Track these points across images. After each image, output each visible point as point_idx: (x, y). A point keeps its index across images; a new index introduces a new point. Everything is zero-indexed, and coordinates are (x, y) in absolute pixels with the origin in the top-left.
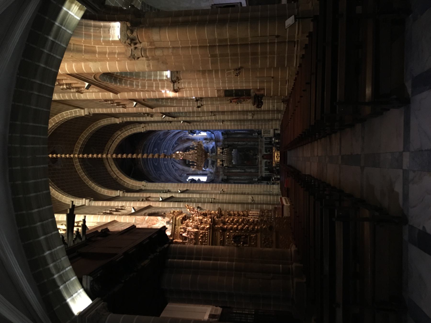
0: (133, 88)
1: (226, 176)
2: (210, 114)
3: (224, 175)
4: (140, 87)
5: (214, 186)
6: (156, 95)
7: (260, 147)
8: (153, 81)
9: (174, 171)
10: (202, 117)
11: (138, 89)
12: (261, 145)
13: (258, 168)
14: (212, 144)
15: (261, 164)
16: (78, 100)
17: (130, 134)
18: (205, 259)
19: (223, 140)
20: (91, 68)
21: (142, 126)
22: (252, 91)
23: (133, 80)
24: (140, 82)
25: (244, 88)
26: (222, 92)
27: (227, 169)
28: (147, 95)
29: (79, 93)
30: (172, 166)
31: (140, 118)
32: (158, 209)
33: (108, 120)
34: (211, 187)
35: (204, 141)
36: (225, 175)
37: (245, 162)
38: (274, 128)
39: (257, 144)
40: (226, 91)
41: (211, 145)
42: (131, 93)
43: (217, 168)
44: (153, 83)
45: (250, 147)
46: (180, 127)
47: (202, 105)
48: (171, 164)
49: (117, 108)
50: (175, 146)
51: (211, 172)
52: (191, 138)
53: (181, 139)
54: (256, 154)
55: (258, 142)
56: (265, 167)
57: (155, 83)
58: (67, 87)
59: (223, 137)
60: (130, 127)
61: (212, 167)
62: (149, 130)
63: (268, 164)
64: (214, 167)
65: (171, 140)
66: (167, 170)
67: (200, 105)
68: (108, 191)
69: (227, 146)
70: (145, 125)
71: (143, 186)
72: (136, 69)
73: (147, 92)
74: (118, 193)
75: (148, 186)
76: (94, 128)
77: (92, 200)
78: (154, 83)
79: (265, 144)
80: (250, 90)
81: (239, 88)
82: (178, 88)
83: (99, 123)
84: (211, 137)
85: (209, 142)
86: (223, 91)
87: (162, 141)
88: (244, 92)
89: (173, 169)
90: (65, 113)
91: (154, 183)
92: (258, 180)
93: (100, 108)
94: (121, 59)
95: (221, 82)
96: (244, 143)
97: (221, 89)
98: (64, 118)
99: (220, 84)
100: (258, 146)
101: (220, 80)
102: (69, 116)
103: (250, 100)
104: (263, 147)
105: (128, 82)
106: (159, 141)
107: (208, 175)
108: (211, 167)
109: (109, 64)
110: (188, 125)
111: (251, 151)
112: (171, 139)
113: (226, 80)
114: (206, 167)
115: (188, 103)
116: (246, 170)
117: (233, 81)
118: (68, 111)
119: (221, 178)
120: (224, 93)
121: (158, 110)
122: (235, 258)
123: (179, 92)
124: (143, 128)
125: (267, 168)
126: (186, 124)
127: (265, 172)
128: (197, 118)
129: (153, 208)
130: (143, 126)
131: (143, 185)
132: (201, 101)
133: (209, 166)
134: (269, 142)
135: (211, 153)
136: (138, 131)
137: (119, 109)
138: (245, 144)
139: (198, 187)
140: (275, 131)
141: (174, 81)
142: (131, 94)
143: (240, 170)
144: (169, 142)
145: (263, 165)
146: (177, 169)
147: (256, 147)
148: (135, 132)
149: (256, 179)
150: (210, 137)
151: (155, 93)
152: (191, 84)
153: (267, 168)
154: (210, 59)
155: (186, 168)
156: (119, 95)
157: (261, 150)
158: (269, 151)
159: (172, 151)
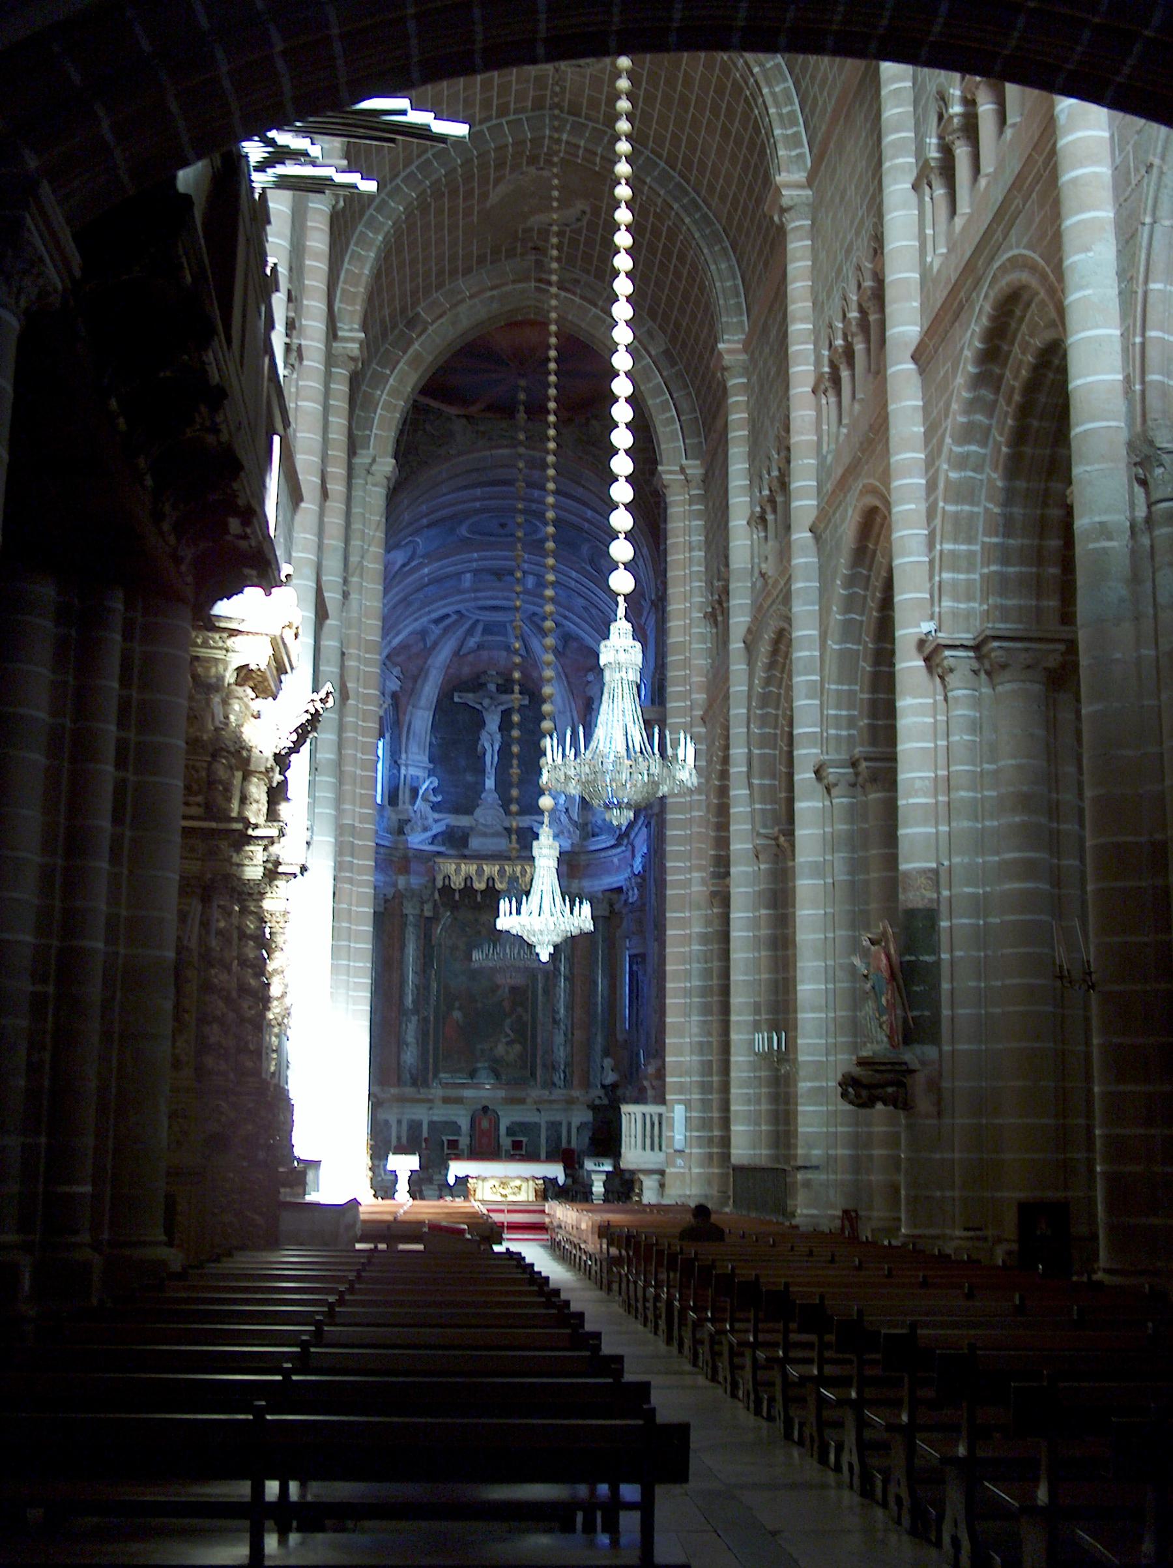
0: (948, 440)
2: (762, 831)
4: (953, 475)
5: (360, 843)
6: (910, 554)
7: (535, 1093)
8: (983, 543)
9: (416, 625)
10: (750, 786)
11: (945, 466)
12: (551, 1102)
15: (446, 1100)
16: (880, 163)
17: (650, 402)
18: (120, 788)
20: (1088, 250)
21: (690, 467)
22: (930, 1052)
23: (991, 441)
24: (979, 477)
25: (946, 1012)
26: (923, 897)
27: (421, 916)
28: (913, 506)
29: (914, 174)
30: (447, 616)
31: (746, 456)
32: (285, 540)
33: (738, 296)
34: (357, 824)
36: (386, 901)
37: (457, 1015)
38: (668, 1171)
39: (556, 1079)
40: (930, 916)
42: (922, 430)
43: (427, 858)
44: (976, 544)
45: (539, 1040)
46: (686, 663)
47: (828, 790)
48: (458, 612)
49: (817, 350)
51: (407, 829)
54: (497, 1075)
55: (568, 1083)
56: (432, 1124)
57: (972, 554)
58: (956, 120)
60: (685, 405)
61: (434, 832)
62: (668, 500)
63: (444, 1138)
64: (432, 843)
65: (585, 615)
66: (427, 585)
67: (831, 779)
68: (364, 280)
70: (694, 484)
71: (368, 461)
72: (1088, 468)
73: (923, 507)
74: (351, 330)
75: (369, 487)
76: (695, 222)
77: (337, 202)
78: (973, 548)
79: (554, 1126)
80: (935, 1040)
81: (945, 986)
82: (951, 670)
83: (717, 248)
84: (597, 830)
85: (570, 818)
86: (931, 900)
87: (589, 568)
88: (927, 1013)
89: (425, 619)
90: (787, 90)
91: (384, 520)
93: (815, 260)
94: (1138, 397)
95: (981, 891)
96: (562, 1011)
97: (939, 893)
98: (762, 84)
99: (967, 885)
100: (543, 1088)
101: (988, 889)
102: (772, 111)
103: (885, 1039)
104: (538, 1110)
105: (979, 418)
106: (585, 549)
108: (437, 829)
109: (1111, 336)
110: (691, 708)
111: (517, 1047)
112: (594, 611)
113: (991, 920)
115: (844, 713)
116: (414, 1019)
117: (986, 956)
118: (797, 107)
120: (920, 906)
121: (804, 558)
122: (122, 951)
123: (924, 671)
124: (682, 470)
125: (425, 1134)
126: (700, 697)
127: (399, 1122)
128: (744, 760)
129: (289, 515)
130: (688, 472)
131: (374, 460)
132: (853, 785)
133: (437, 816)
134: (564, 1145)
135: (506, 829)
136: (663, 446)
137: (812, 359)
139: (359, 755)
140: (656, 1177)
141: (985, 650)
142: (915, 429)
144: (582, 602)
145: (441, 1113)
146: (428, 645)
147: (539, 1072)
148: (660, 429)
151: (923, 548)
152: (966, 737)
153: (425, 1134)
154: (1143, 839)
155: (430, 690)
156: (911, 366)
157: (522, 1101)
158: (517, 1145)
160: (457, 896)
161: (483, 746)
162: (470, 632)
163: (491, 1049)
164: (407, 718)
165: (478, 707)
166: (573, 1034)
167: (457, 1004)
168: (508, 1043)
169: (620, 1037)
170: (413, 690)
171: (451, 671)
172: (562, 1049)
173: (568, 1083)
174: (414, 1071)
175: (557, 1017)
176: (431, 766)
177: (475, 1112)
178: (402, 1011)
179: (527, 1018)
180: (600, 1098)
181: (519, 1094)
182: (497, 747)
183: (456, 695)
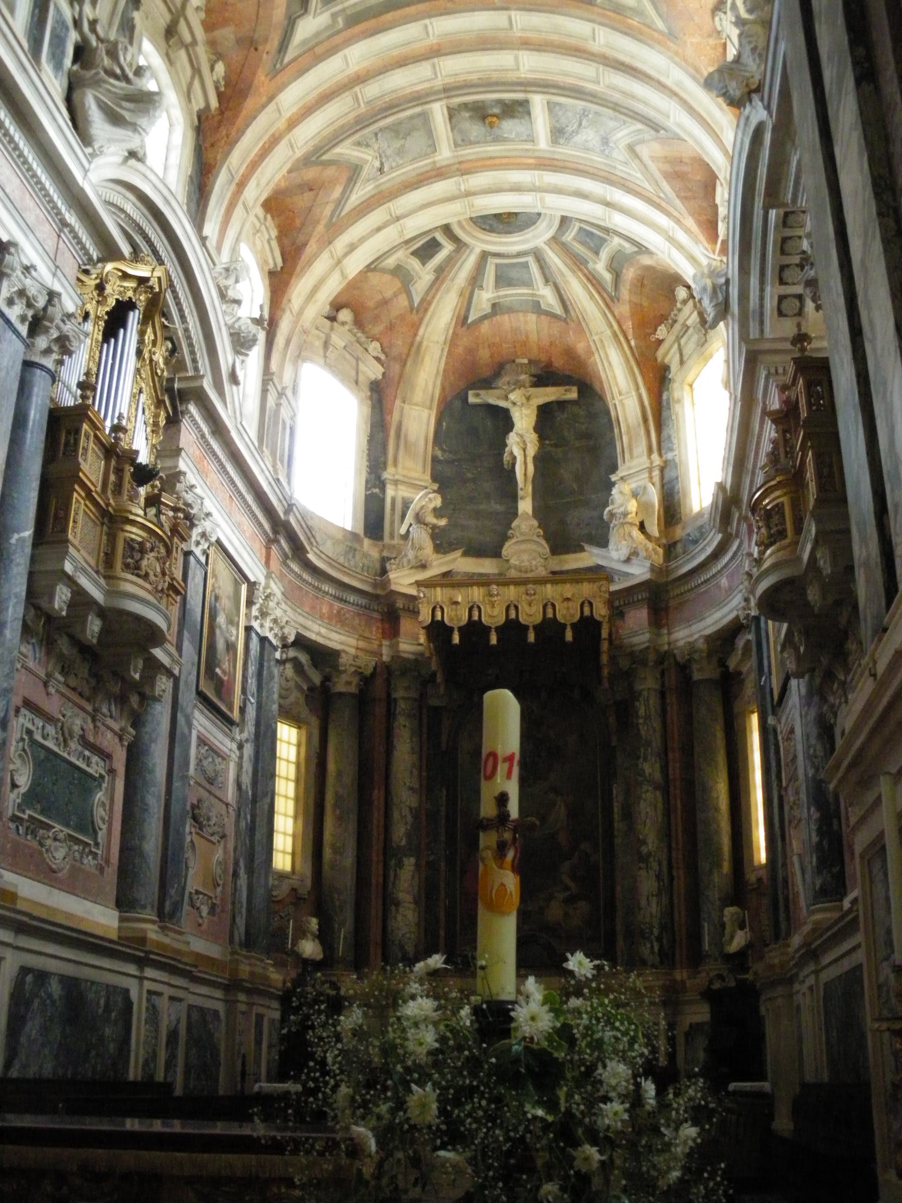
1: (353, 689)
3: (368, 672)
14: (628, 560)
35: (654, 495)
41: (624, 553)
48: (447, 229)
50: (600, 266)
52: (676, 395)
53: (662, 318)
59: (701, 645)
92: (308, 966)
107: (367, 542)
111: (583, 906)
114: (431, 519)
116: (409, 863)
138: (644, 842)
146: (417, 300)
149: (309, 948)
159: (556, 240)
161: (511, 453)
162: (476, 280)
164: (396, 416)
165: (502, 404)
166: (671, 879)
168: (570, 900)
169: (752, 877)
170: (401, 376)
171: (460, 350)
172: (654, 901)
173: (667, 959)
175: (644, 850)
176: (436, 486)
178: (389, 852)
180: (721, 977)
182: (532, 451)
183: (471, 393)
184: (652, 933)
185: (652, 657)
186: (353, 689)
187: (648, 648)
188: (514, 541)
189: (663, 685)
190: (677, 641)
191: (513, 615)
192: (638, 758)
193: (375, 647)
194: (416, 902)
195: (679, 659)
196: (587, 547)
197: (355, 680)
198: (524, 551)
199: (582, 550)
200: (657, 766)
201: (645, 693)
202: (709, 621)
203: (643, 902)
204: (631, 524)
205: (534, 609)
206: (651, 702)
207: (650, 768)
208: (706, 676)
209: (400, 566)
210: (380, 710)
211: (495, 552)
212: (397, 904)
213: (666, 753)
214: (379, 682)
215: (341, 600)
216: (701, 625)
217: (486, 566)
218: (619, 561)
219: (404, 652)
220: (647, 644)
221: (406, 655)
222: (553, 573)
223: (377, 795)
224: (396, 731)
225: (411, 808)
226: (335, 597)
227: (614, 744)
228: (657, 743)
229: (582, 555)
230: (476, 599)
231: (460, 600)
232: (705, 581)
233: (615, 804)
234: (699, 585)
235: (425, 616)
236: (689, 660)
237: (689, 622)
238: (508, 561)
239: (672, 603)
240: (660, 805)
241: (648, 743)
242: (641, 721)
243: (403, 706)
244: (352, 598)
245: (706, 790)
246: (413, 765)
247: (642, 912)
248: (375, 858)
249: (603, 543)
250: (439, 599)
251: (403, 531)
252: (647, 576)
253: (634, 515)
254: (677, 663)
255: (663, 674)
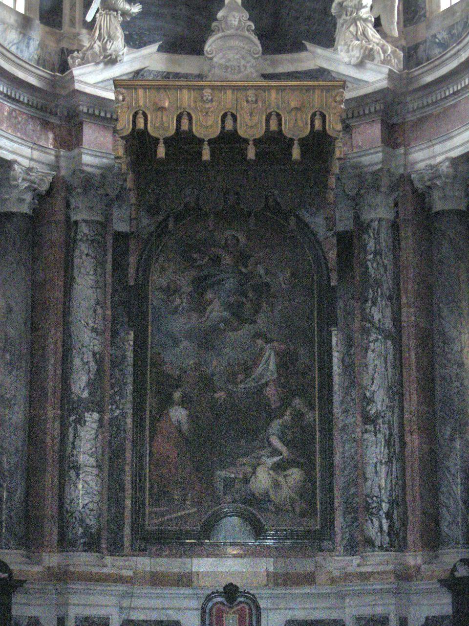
1: (25, 209)
3: (44, 188)
12: (364, 577)
13: (116, 548)
14: (360, 65)
19: (405, 180)
37: (178, 414)
59: (445, 168)
69: (340, 227)
100: (352, 548)
111: (295, 475)
119: (9, 157)
138: (370, 401)
143: (99, 359)
147: (339, 521)
150: (443, 35)
157: (309, 579)
160: (161, 152)
163: (246, 481)
166: (403, 444)
167: (177, 395)
168: (279, 467)
172: (383, 469)
174: (91, 521)
177: (209, 598)
179: (313, 417)
181: (303, 565)
184: (380, 508)
185: (385, 181)
186: (25, 209)
187: (381, 170)
188: (220, 34)
189: (397, 216)
190: (416, 163)
191: (229, 125)
192: (366, 301)
193: (53, 158)
194: (99, 466)
195: (418, 185)
196: (308, 45)
197: (28, 197)
198: (230, 48)
199: (305, 49)
200: (388, 312)
201: (376, 224)
202: (458, 140)
203: (370, 470)
204: (365, 20)
205: (256, 119)
206: (382, 235)
207: (380, 313)
208: (449, 206)
209: (84, 61)
210: (55, 234)
211: (196, 49)
212: (77, 468)
213: (399, 298)
214: (59, 203)
215: (14, 100)
216: (449, 144)
217: (188, 64)
218: (349, 64)
219: (88, 165)
220: (380, 166)
221: (89, 170)
222: (265, 77)
223: (54, 337)
224: (77, 261)
225: (94, 354)
226: (6, 95)
227: (333, 283)
228: (388, 284)
229: (303, 54)
230: (185, 105)
231: (167, 105)
232: (454, 93)
233: (335, 354)
234: (446, 98)
235: (125, 124)
236: (429, 187)
237: (431, 141)
238: (211, 59)
239: (411, 118)
240: (390, 357)
241: (379, 284)
242: (370, 257)
243: (87, 232)
244: (24, 98)
245: (447, 340)
246: (98, 303)
247: (369, 483)
248: (50, 413)
249: (328, 40)
250: (142, 103)
251: (89, 18)
252: (384, 84)
253: (368, 9)
254: (415, 191)
255: (396, 205)
